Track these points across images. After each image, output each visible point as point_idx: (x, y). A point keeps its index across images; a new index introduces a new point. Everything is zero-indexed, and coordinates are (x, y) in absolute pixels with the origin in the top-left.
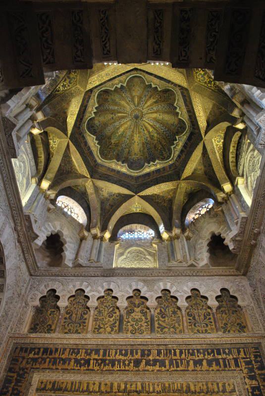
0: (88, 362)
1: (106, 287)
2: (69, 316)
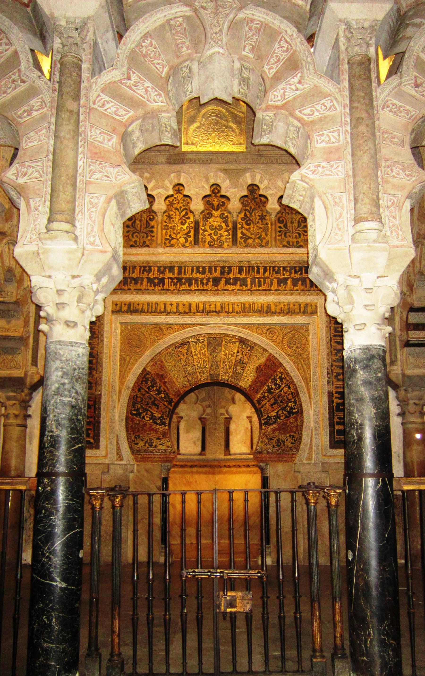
0: (162, 281)
1: (176, 181)
2: (132, 224)
